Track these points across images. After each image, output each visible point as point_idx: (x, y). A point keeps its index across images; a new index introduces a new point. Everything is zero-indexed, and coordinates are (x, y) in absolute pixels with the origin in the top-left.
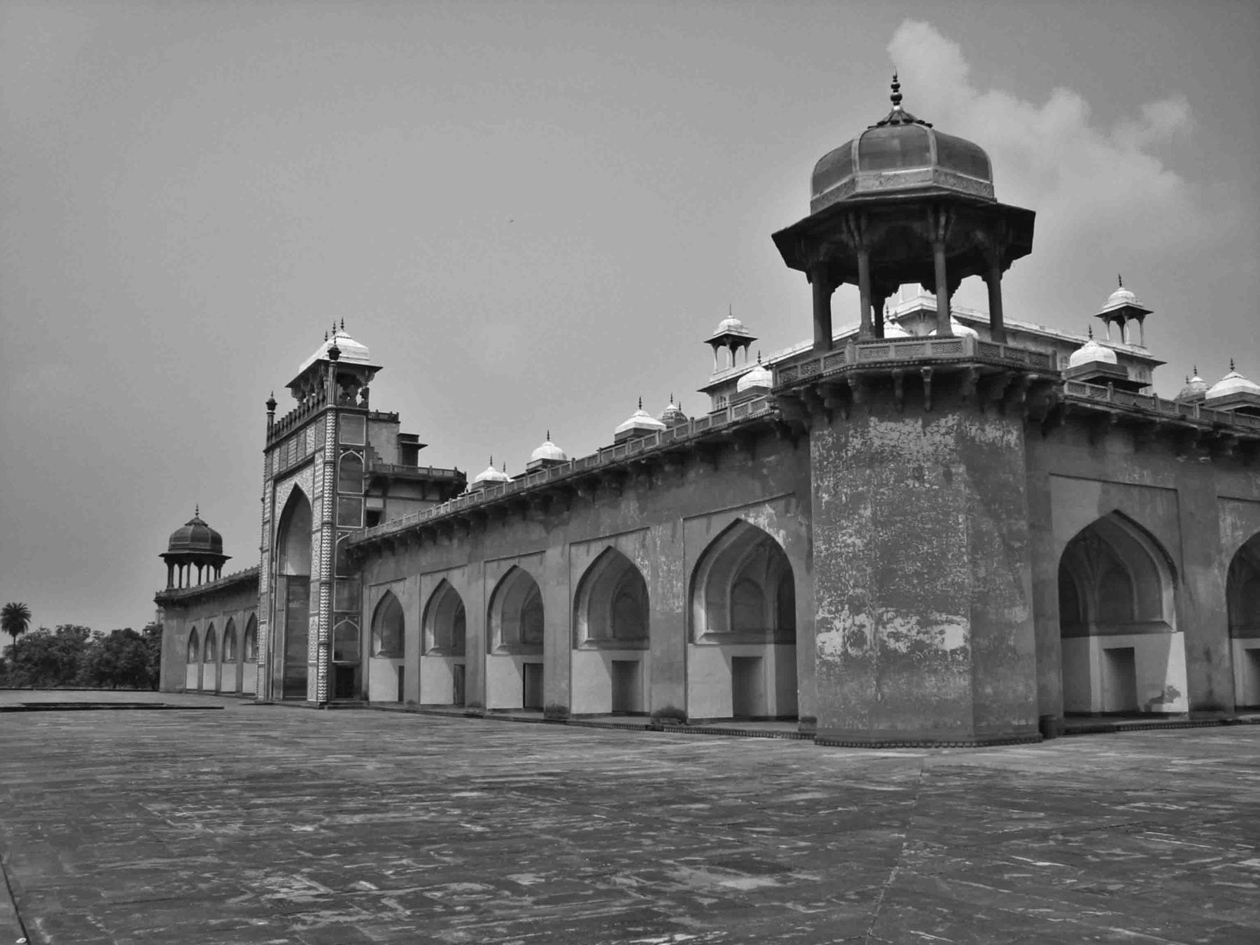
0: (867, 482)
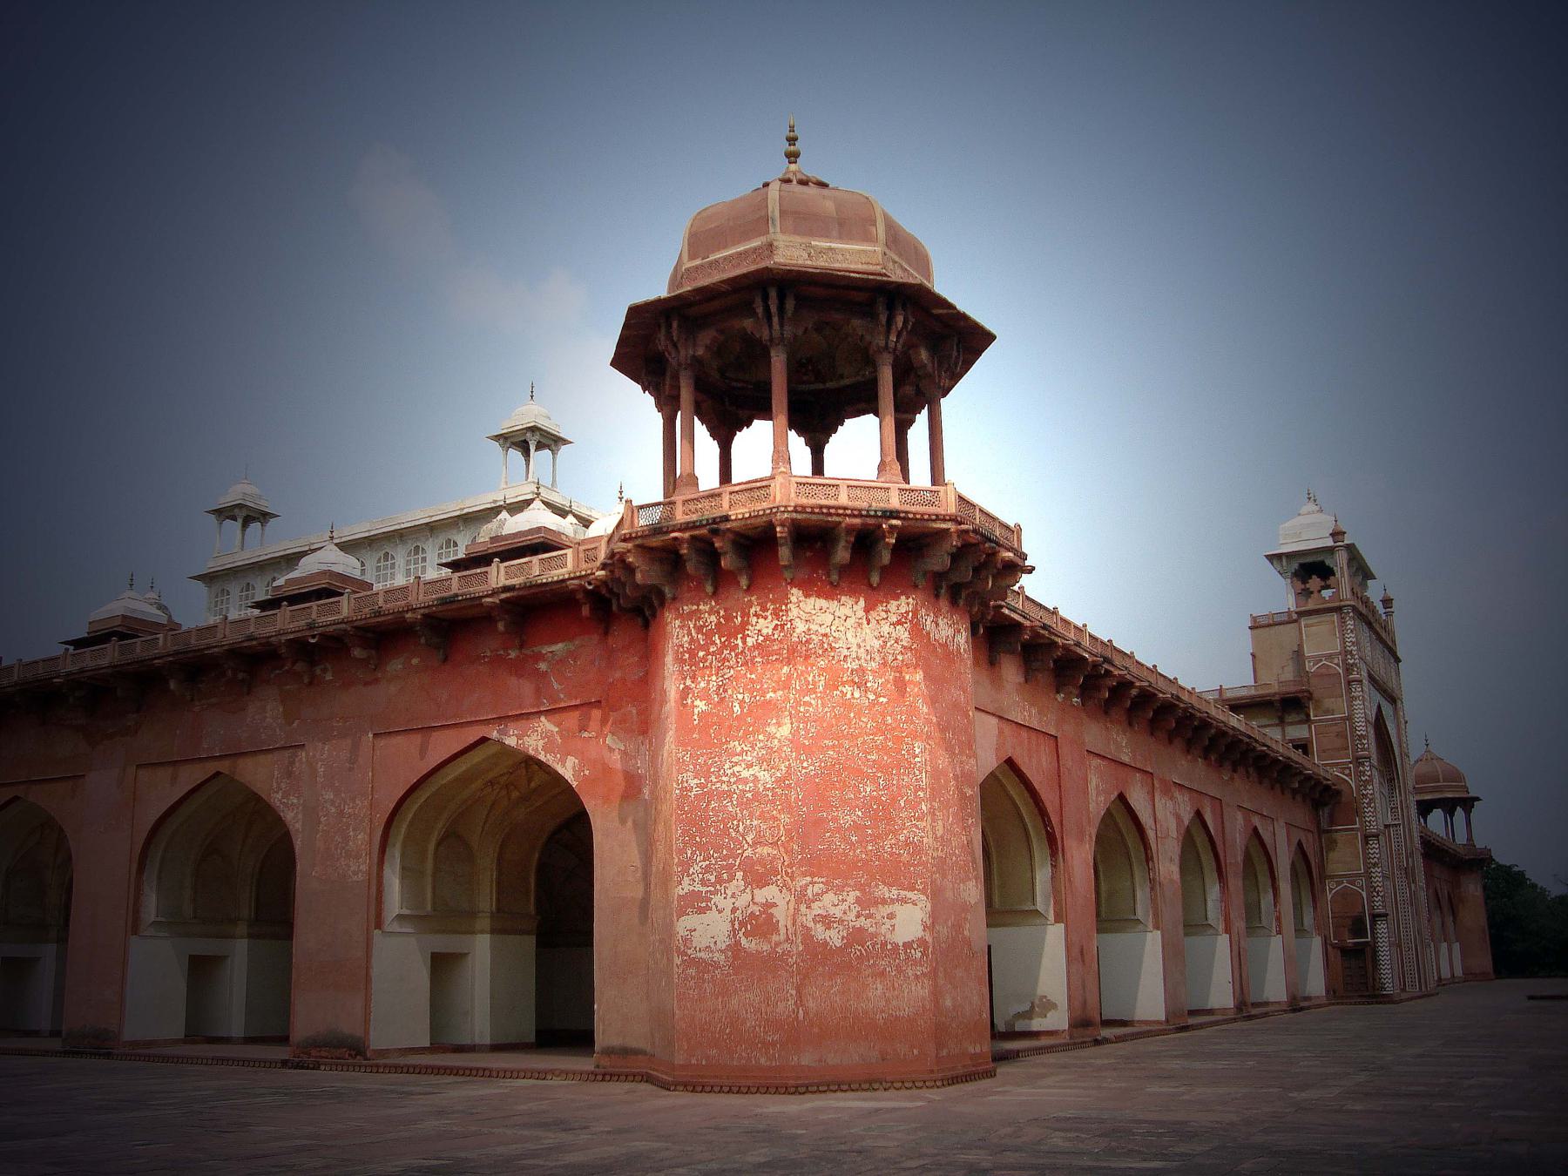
0: (786, 686)
